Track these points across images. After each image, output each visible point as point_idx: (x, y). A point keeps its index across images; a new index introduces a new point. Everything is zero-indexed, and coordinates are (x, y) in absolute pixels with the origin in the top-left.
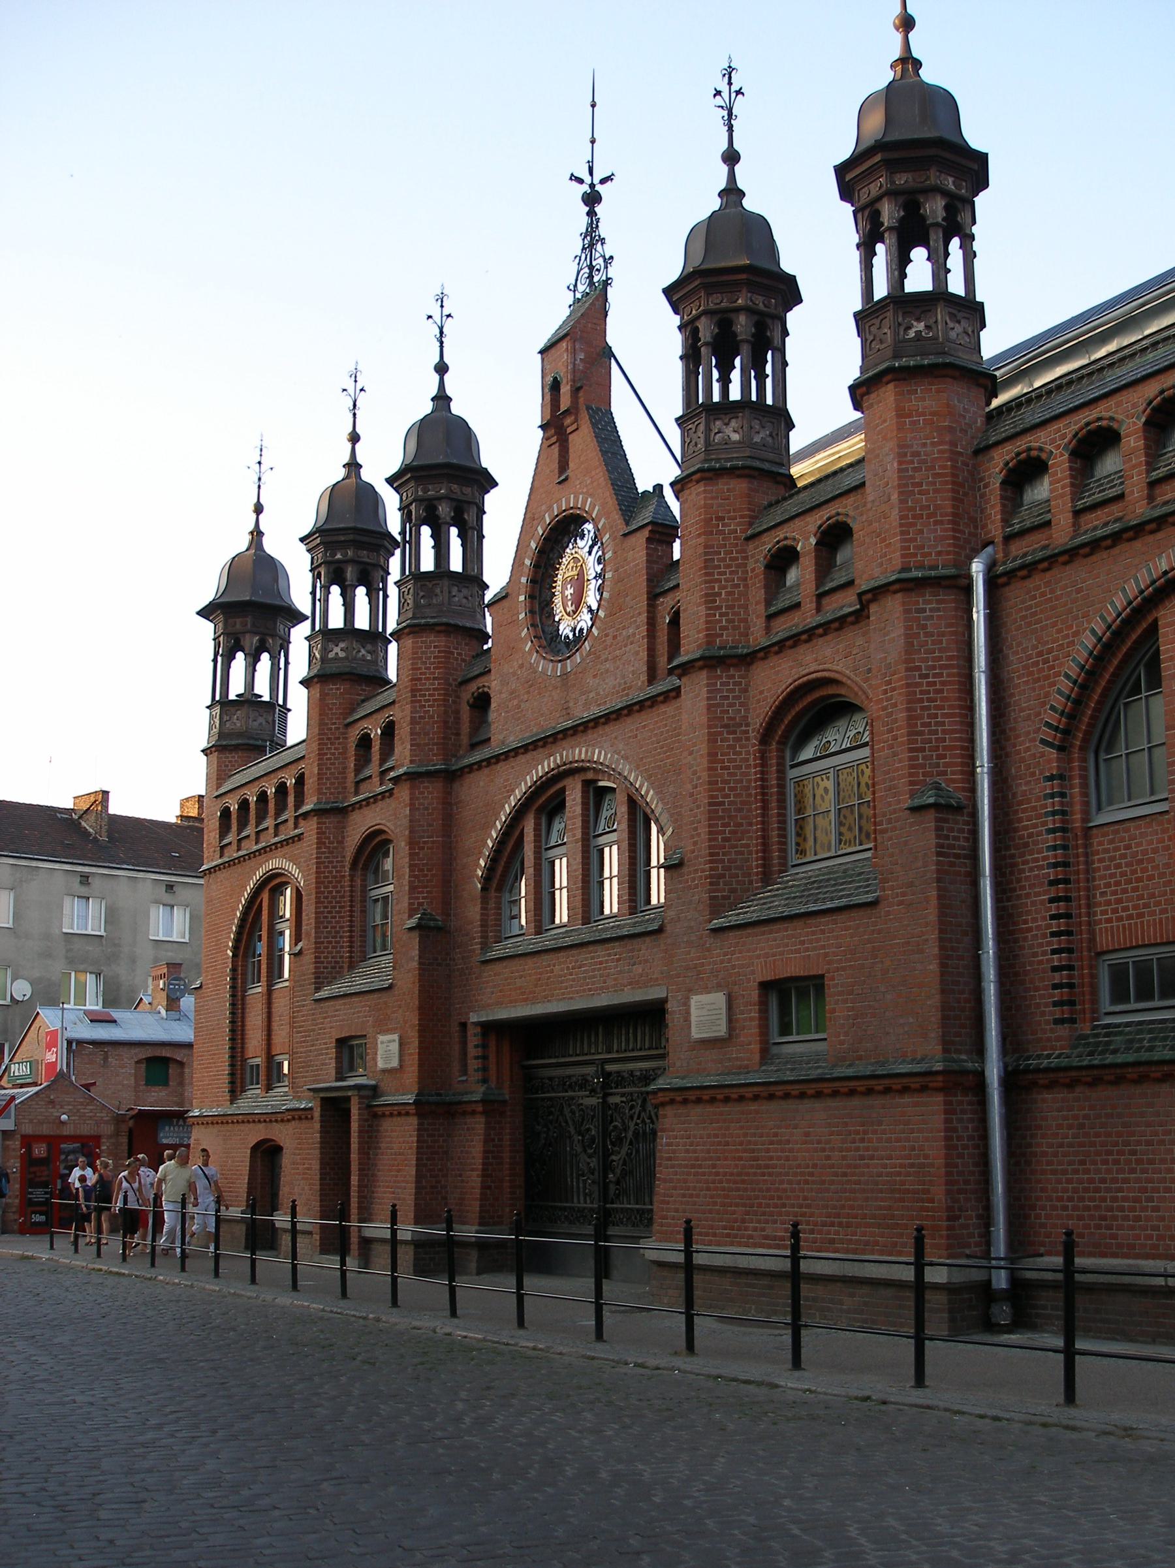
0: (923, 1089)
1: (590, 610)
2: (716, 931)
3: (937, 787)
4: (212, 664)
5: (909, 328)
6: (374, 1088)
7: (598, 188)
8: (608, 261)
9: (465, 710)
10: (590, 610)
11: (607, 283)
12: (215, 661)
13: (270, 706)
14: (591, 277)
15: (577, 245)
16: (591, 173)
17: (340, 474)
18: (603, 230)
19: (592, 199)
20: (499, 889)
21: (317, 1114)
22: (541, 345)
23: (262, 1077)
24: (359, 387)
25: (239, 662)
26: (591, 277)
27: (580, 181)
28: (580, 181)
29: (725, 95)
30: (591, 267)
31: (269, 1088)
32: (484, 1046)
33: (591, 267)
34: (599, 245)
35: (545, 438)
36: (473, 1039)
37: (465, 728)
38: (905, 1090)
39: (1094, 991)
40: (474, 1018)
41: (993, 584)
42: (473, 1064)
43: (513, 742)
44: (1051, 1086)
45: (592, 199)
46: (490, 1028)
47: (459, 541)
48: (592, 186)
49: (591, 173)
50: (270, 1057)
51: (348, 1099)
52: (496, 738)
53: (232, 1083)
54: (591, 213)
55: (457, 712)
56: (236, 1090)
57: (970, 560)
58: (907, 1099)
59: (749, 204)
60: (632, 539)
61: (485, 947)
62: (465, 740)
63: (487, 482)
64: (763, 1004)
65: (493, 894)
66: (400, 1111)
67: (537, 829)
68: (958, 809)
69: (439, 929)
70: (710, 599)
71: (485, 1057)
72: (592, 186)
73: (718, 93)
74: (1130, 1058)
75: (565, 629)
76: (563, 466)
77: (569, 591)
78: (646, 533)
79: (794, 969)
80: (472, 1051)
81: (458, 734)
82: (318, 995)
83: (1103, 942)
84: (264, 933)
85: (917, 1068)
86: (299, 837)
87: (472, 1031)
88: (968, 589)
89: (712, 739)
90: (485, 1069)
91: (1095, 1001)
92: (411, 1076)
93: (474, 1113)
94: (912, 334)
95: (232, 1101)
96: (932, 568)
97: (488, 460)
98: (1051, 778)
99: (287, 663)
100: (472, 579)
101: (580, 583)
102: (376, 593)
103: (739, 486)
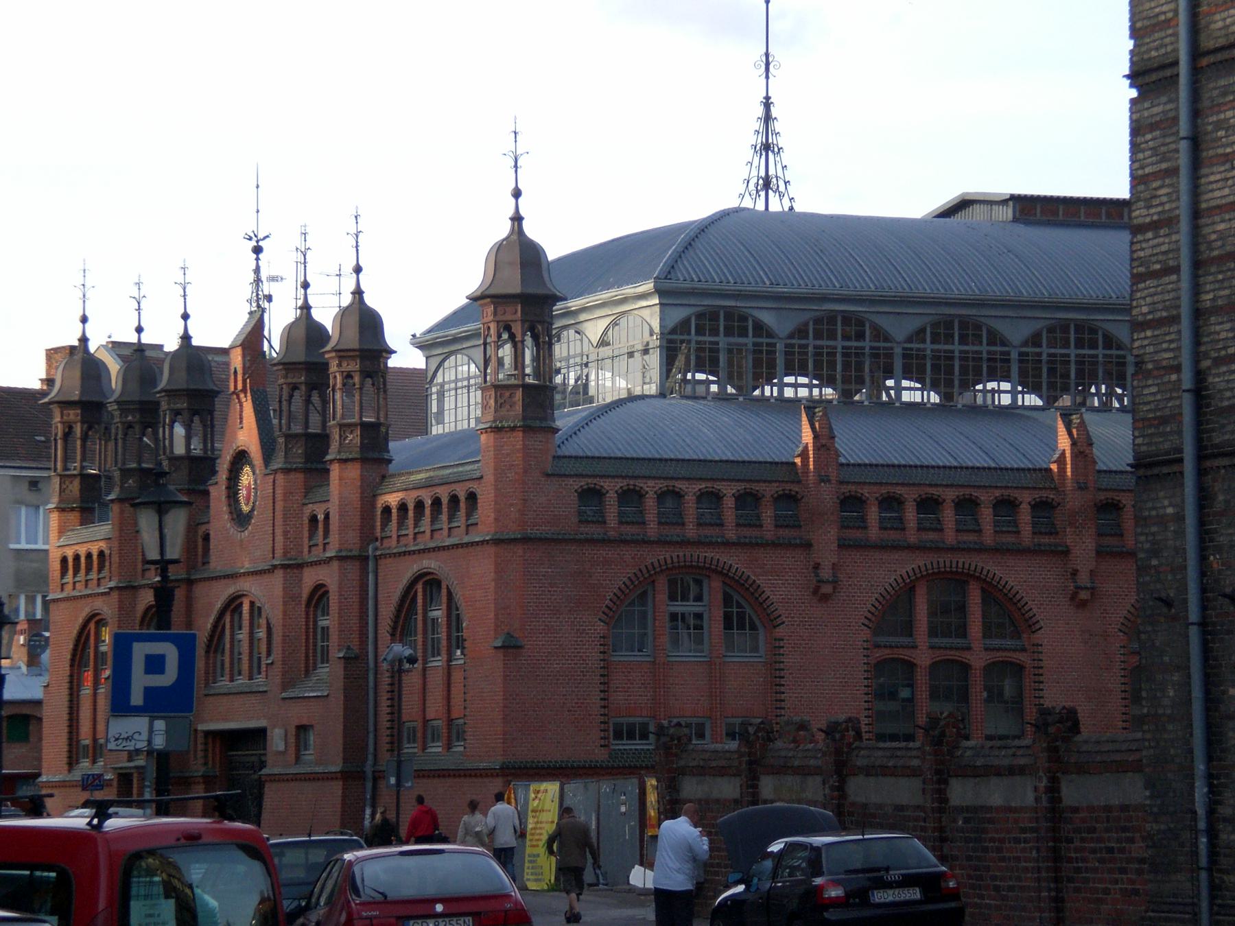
2: (284, 699)
20: (216, 651)
21: (115, 783)
32: (206, 744)
36: (200, 740)
40: (201, 727)
42: (200, 754)
46: (208, 733)
51: (131, 774)
53: (70, 757)
55: (196, 541)
56: (72, 763)
60: (267, 477)
61: (207, 684)
65: (212, 655)
67: (232, 621)
89: (285, 604)
90: (206, 757)
93: (199, 783)
95: (69, 771)
96: (351, 551)
103: (301, 476)
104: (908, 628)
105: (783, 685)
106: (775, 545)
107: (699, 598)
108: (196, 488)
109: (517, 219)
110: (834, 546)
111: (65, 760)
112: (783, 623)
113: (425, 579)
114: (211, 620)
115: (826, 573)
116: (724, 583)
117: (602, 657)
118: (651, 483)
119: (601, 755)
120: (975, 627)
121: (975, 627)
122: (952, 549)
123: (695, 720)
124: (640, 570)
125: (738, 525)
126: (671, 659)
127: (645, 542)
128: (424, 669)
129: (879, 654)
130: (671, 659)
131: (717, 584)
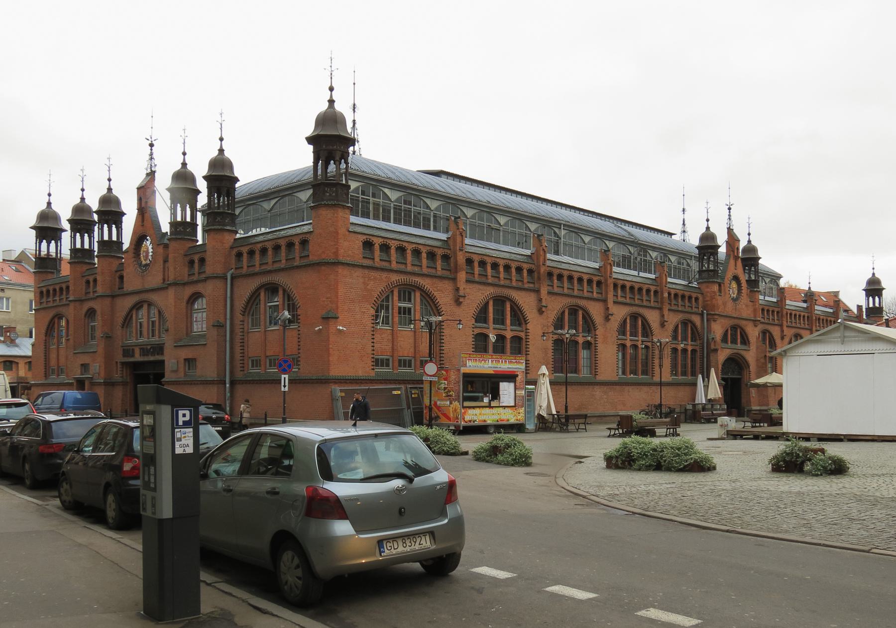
0: (213, 383)
1: (150, 261)
2: (175, 346)
3: (218, 321)
4: (35, 244)
5: (217, 219)
6: (92, 378)
7: (154, 142)
8: (155, 165)
9: (117, 280)
10: (150, 261)
11: (155, 172)
12: (36, 243)
13: (55, 259)
14: (151, 168)
15: (148, 157)
16: (151, 138)
17: (78, 201)
18: (154, 156)
19: (151, 145)
21: (75, 384)
22: (137, 186)
23: (56, 372)
24: (84, 175)
25: (44, 243)
26: (151, 168)
27: (148, 140)
28: (148, 140)
29: (183, 137)
30: (151, 165)
31: (58, 375)
33: (151, 165)
34: (153, 160)
35: (138, 212)
36: (119, 366)
37: (117, 283)
38: (210, 384)
39: (248, 365)
41: (233, 278)
43: (131, 289)
44: (239, 383)
45: (151, 145)
47: (115, 229)
48: (152, 141)
49: (151, 138)
50: (58, 367)
51: (84, 380)
52: (125, 289)
54: (151, 150)
56: (46, 376)
57: (228, 272)
58: (210, 385)
59: (189, 167)
62: (117, 287)
63: (123, 214)
64: (185, 365)
66: (99, 384)
68: (223, 326)
69: (110, 337)
70: (175, 268)
71: (122, 371)
72: (152, 141)
73: (181, 136)
74: (251, 379)
75: (144, 262)
76: (143, 221)
77: (144, 254)
78: (162, 246)
79: (190, 357)
80: (119, 369)
81: (115, 285)
82: (75, 352)
83: (250, 356)
84: (56, 330)
85: (212, 379)
86: (68, 304)
87: (119, 364)
88: (227, 279)
91: (248, 367)
92: (102, 374)
94: (217, 220)
97: (124, 208)
98: (241, 321)
99: (61, 245)
100: (119, 243)
101: (147, 252)
102: (91, 237)
104: (485, 321)
105: (443, 343)
106: (441, 278)
107: (410, 300)
108: (115, 255)
109: (331, 102)
110: (464, 281)
111: (44, 375)
112: (444, 314)
113: (267, 287)
114: (124, 313)
115: (461, 293)
116: (421, 294)
117: (372, 325)
118: (393, 242)
119: (372, 374)
120: (508, 322)
121: (508, 322)
122: (503, 286)
123: (408, 358)
124: (389, 284)
125: (427, 267)
126: (399, 329)
127: (391, 271)
128: (265, 331)
129: (477, 331)
130: (399, 329)
131: (418, 294)
